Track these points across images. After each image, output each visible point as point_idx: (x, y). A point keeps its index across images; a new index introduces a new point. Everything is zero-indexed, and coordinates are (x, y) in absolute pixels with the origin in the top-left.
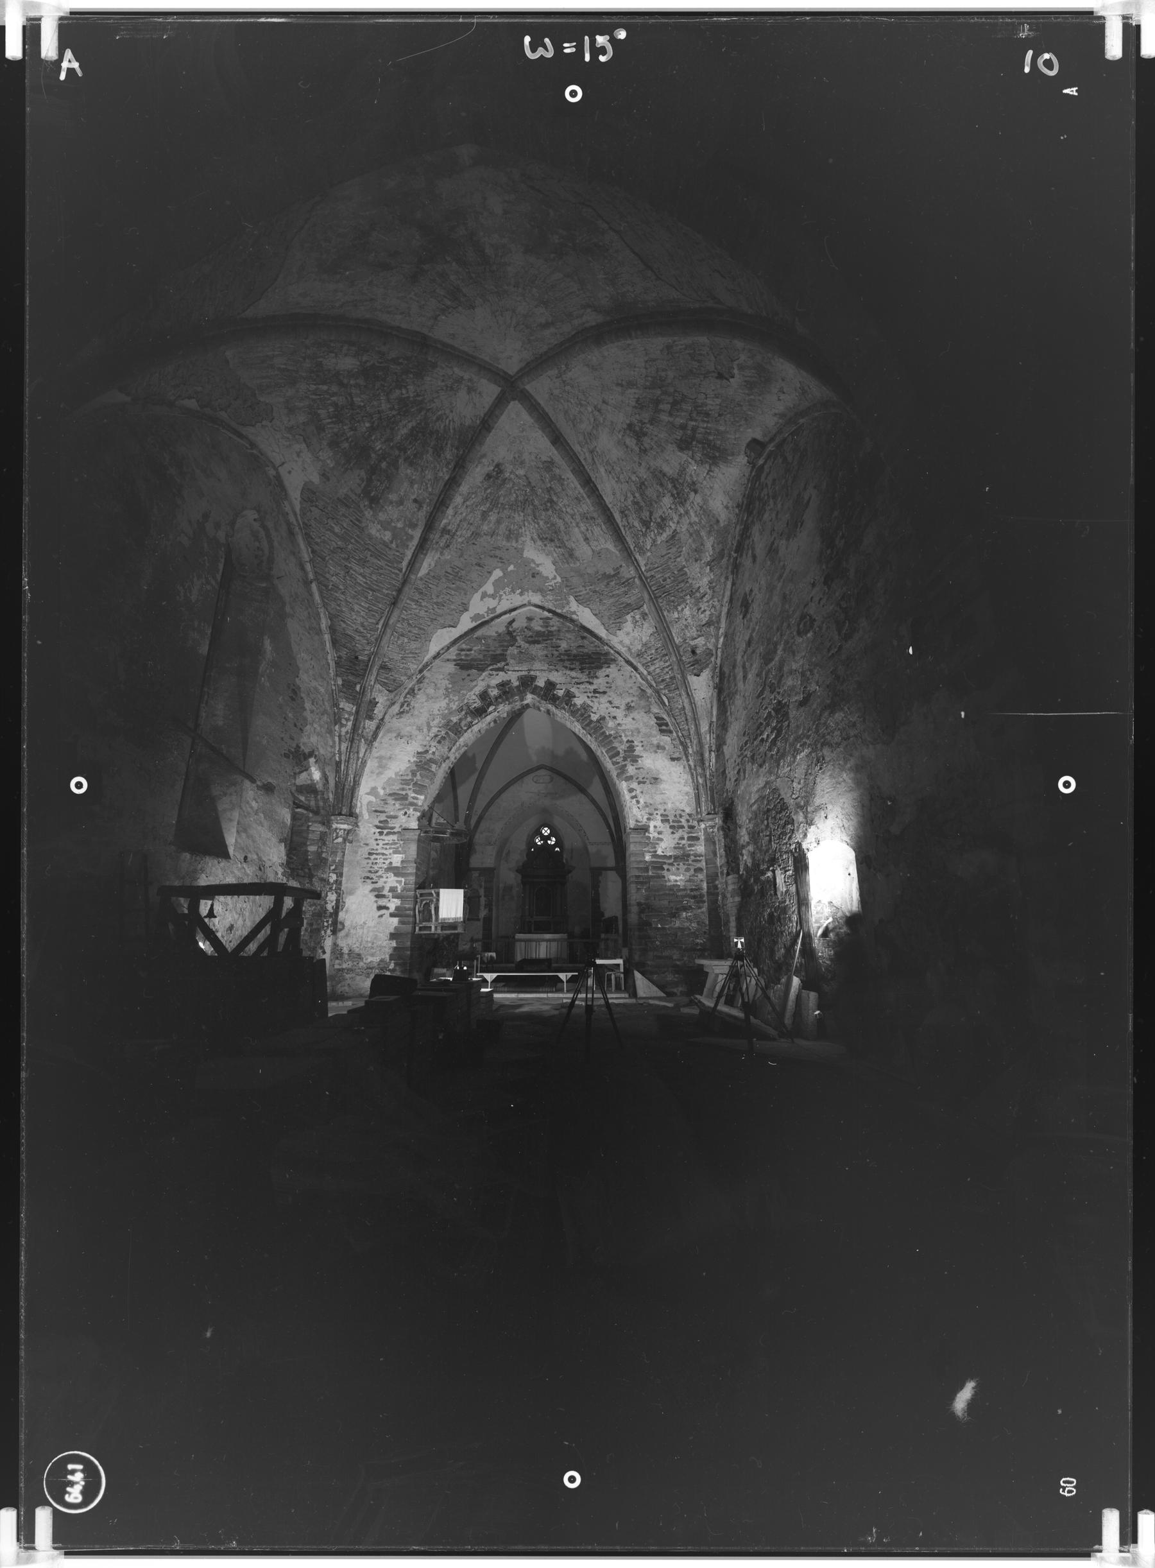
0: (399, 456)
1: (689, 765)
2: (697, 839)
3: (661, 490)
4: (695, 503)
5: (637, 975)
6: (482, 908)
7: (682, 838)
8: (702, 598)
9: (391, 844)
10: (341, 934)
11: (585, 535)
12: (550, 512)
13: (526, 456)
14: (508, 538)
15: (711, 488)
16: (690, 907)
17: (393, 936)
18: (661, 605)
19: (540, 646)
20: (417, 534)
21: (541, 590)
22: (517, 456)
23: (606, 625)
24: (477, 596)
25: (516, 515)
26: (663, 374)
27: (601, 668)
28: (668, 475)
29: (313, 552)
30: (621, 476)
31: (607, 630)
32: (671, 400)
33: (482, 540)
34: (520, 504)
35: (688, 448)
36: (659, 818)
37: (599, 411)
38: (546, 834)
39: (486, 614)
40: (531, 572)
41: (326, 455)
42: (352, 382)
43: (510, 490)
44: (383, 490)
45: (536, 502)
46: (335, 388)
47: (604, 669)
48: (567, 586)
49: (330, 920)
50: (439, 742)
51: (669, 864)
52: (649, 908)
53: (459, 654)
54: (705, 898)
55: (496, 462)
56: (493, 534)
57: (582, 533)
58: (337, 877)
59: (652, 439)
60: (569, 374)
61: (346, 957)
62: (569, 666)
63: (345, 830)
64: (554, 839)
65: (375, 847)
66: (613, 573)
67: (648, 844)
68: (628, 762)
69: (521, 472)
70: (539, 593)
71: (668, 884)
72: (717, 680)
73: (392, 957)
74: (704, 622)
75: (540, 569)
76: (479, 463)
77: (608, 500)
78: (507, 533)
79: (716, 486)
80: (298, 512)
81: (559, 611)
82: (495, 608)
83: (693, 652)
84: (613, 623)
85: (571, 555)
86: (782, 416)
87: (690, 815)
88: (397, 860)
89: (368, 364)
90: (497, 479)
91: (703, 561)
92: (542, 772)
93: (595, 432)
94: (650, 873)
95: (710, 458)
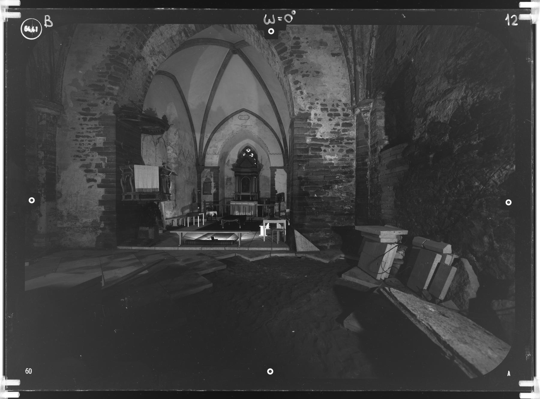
1: (348, 60)
2: (350, 125)
5: (297, 233)
6: (213, 188)
7: (338, 124)
9: (94, 128)
10: (60, 201)
16: (342, 181)
17: (101, 203)
36: (319, 107)
38: (248, 152)
49: (43, 189)
50: (128, 38)
51: (326, 146)
52: (307, 182)
54: (354, 174)
58: (45, 154)
61: (66, 218)
63: (49, 115)
64: (252, 154)
65: (81, 131)
67: (309, 129)
68: (294, 58)
71: (325, 162)
73: (102, 219)
87: (345, 105)
88: (100, 141)
92: (243, 113)
94: (310, 154)
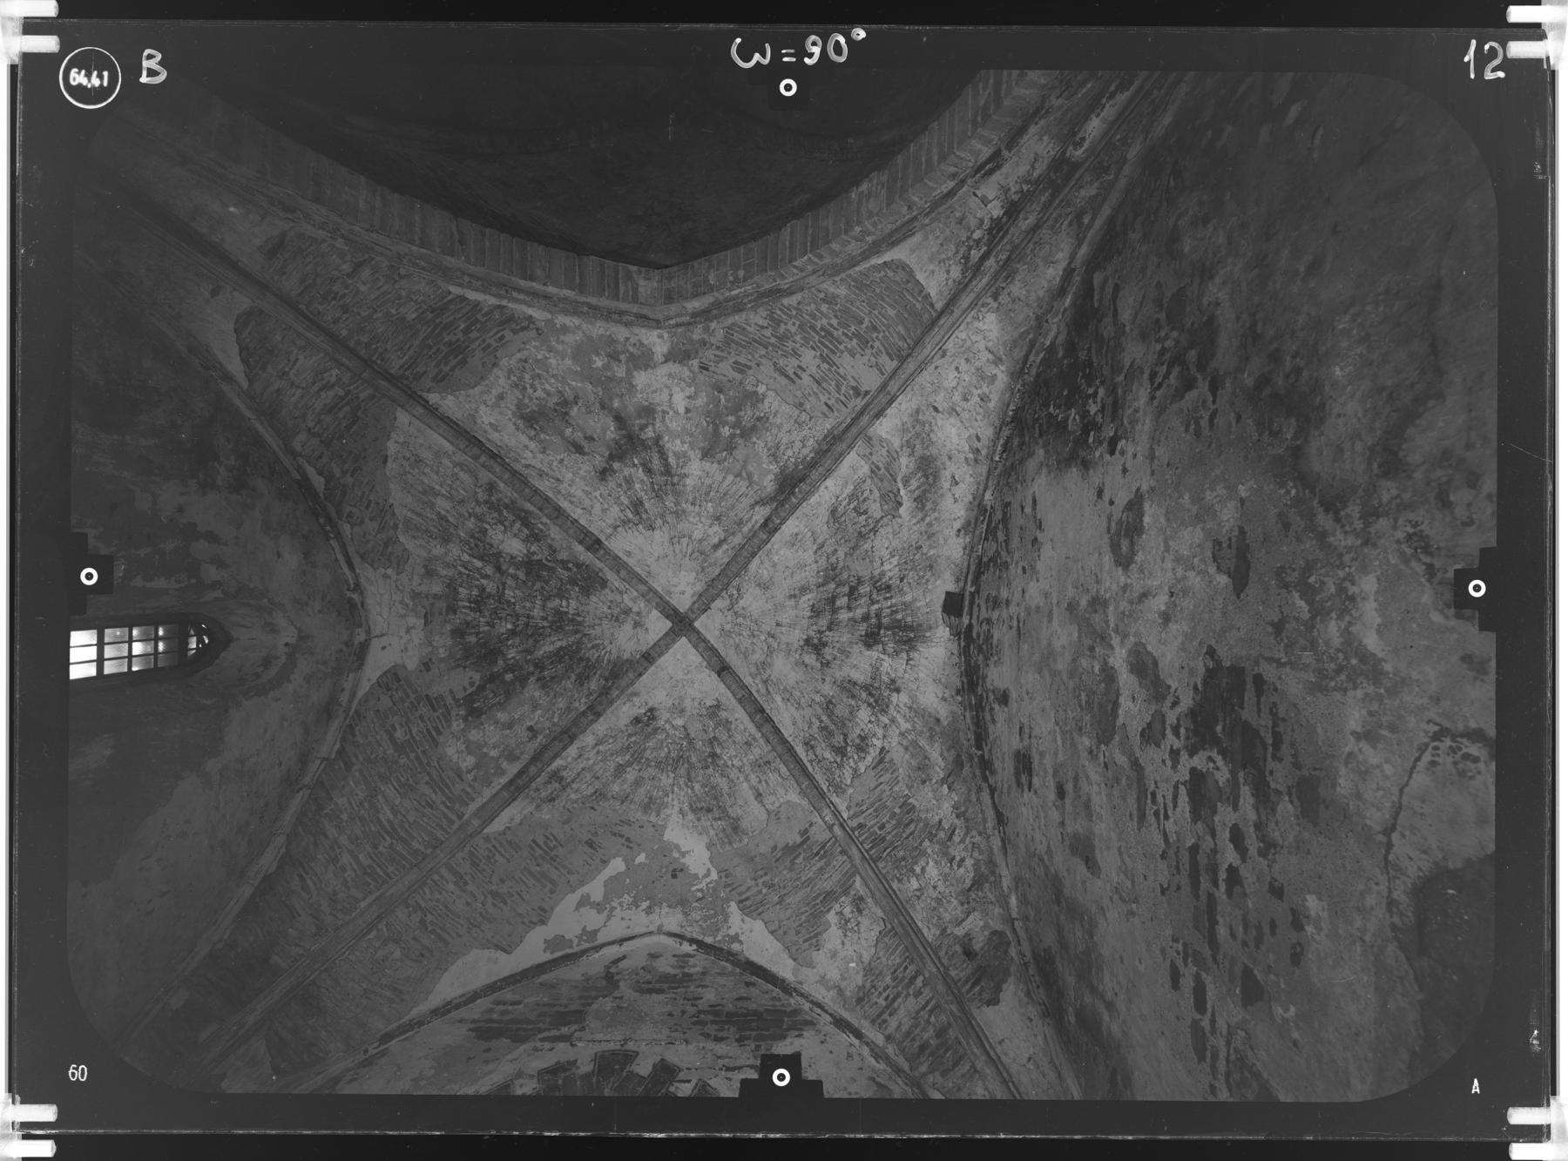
0: (533, 673)
3: (853, 703)
4: (901, 705)
8: (950, 838)
11: (757, 790)
12: (711, 770)
13: (688, 704)
14: (646, 808)
15: (916, 679)
18: (884, 871)
19: (661, 997)
20: (512, 769)
21: (682, 903)
22: (676, 702)
23: (793, 950)
24: (572, 899)
25: (664, 777)
26: (833, 560)
27: (784, 1037)
28: (859, 682)
29: (341, 752)
30: (803, 701)
31: (795, 960)
32: (846, 589)
33: (606, 804)
34: (671, 762)
35: (876, 642)
37: (773, 637)
39: (576, 941)
40: (671, 869)
41: (443, 643)
42: (511, 571)
43: (662, 743)
44: (495, 704)
45: (694, 759)
46: (489, 570)
47: (789, 1040)
48: (727, 886)
53: (491, 1011)
55: (650, 705)
56: (625, 799)
57: (752, 788)
59: (834, 647)
60: (742, 603)
62: (713, 1033)
66: (799, 840)
69: (679, 722)
70: (679, 908)
72: (1041, 994)
74: (968, 883)
75: (687, 860)
76: (629, 700)
77: (787, 732)
78: (646, 800)
79: (922, 675)
80: (360, 694)
81: (709, 940)
82: (596, 931)
83: (969, 953)
84: (805, 941)
85: (736, 829)
86: (966, 528)
89: (535, 558)
90: (648, 726)
91: (934, 781)
93: (769, 660)
95: (905, 643)
